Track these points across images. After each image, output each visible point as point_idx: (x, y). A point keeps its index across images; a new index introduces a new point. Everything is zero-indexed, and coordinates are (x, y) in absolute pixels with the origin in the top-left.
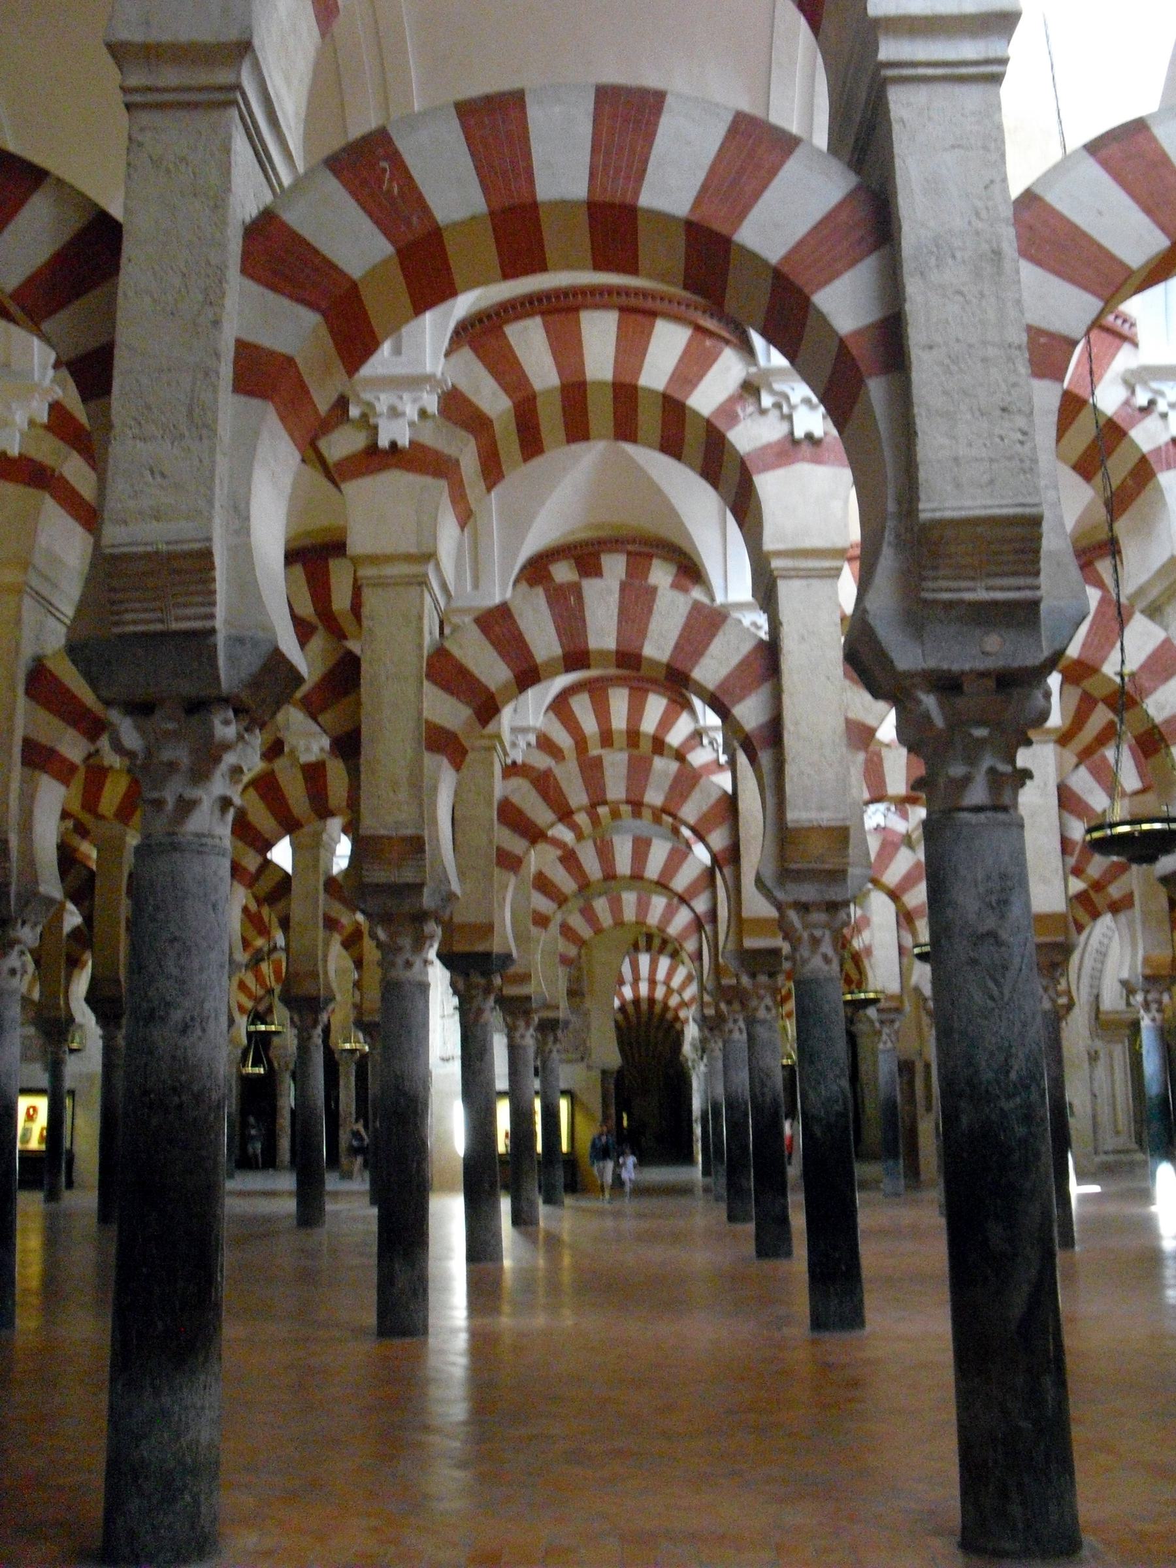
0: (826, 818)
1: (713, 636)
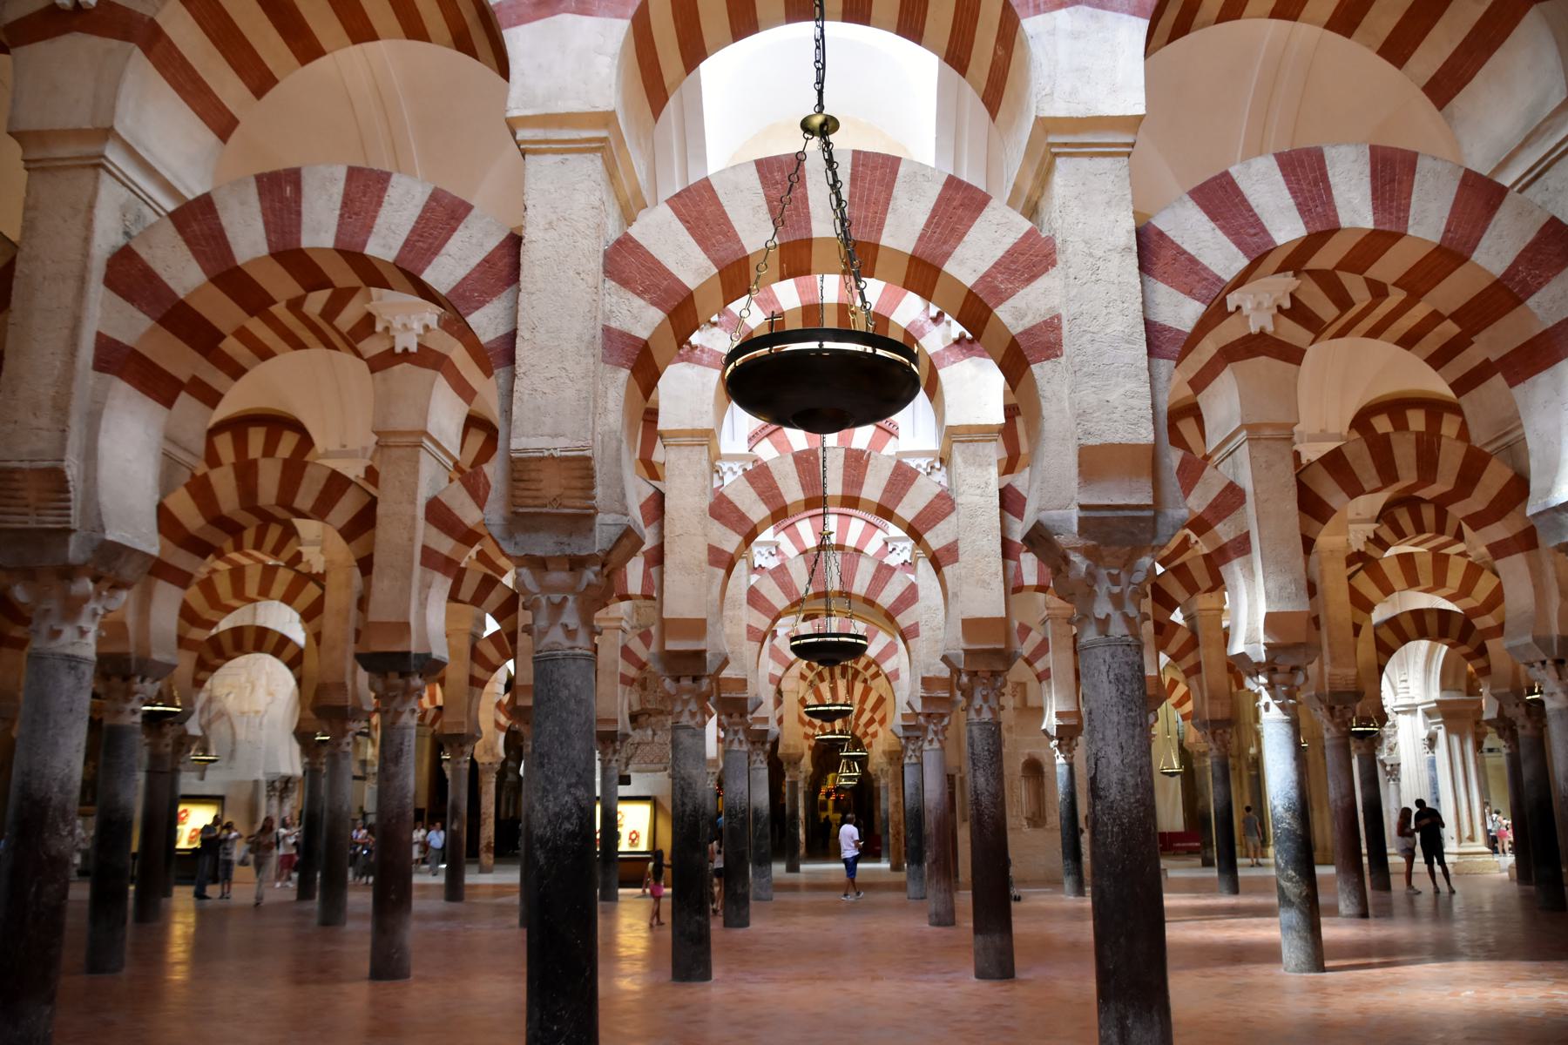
0: (559, 445)
1: (454, 230)
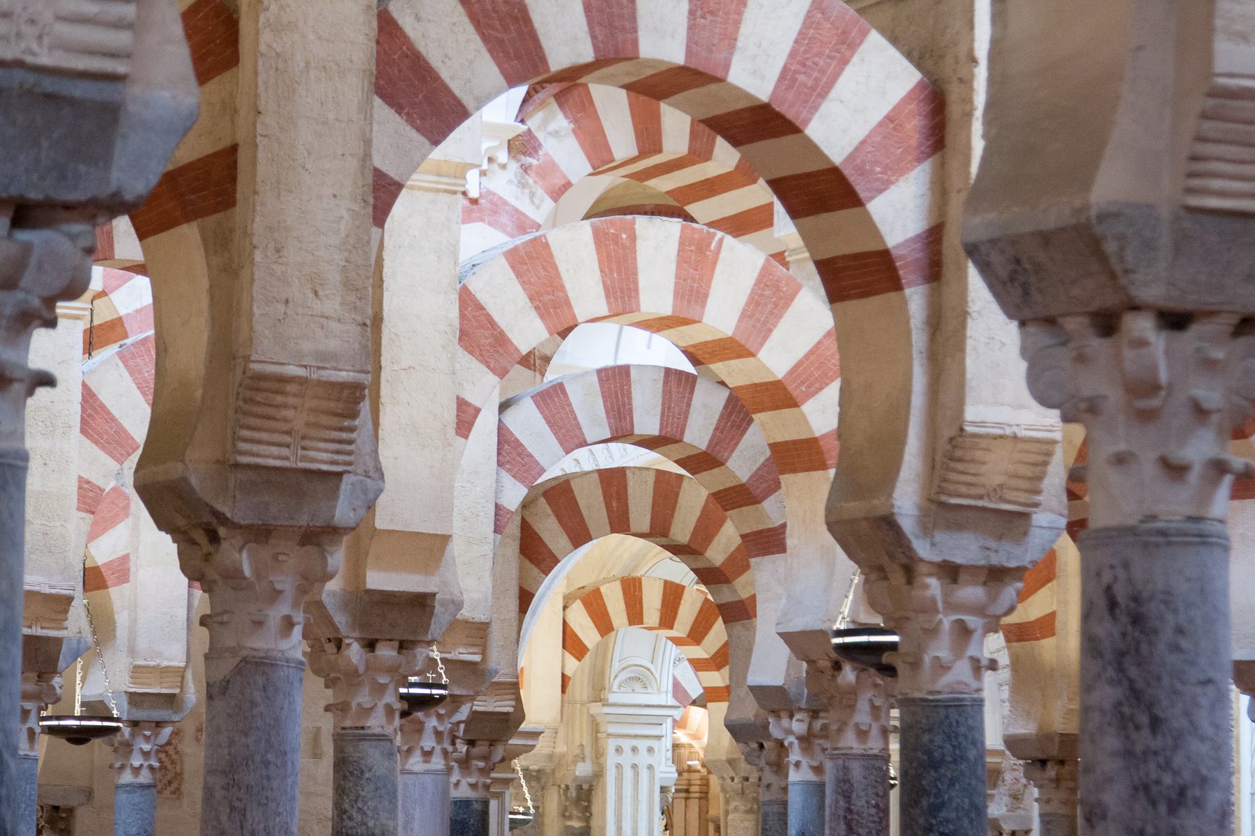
1: (845, 62)
